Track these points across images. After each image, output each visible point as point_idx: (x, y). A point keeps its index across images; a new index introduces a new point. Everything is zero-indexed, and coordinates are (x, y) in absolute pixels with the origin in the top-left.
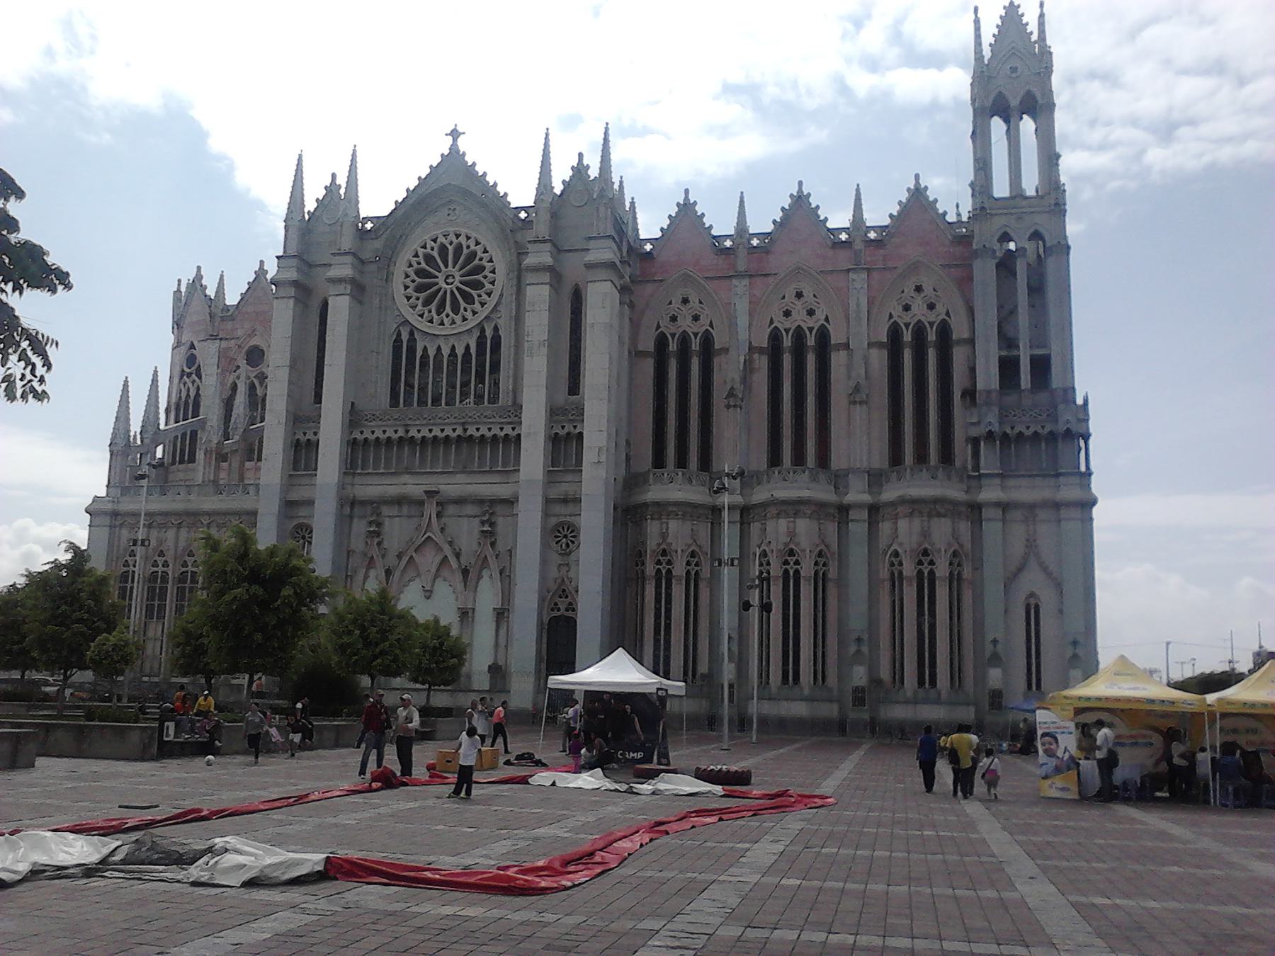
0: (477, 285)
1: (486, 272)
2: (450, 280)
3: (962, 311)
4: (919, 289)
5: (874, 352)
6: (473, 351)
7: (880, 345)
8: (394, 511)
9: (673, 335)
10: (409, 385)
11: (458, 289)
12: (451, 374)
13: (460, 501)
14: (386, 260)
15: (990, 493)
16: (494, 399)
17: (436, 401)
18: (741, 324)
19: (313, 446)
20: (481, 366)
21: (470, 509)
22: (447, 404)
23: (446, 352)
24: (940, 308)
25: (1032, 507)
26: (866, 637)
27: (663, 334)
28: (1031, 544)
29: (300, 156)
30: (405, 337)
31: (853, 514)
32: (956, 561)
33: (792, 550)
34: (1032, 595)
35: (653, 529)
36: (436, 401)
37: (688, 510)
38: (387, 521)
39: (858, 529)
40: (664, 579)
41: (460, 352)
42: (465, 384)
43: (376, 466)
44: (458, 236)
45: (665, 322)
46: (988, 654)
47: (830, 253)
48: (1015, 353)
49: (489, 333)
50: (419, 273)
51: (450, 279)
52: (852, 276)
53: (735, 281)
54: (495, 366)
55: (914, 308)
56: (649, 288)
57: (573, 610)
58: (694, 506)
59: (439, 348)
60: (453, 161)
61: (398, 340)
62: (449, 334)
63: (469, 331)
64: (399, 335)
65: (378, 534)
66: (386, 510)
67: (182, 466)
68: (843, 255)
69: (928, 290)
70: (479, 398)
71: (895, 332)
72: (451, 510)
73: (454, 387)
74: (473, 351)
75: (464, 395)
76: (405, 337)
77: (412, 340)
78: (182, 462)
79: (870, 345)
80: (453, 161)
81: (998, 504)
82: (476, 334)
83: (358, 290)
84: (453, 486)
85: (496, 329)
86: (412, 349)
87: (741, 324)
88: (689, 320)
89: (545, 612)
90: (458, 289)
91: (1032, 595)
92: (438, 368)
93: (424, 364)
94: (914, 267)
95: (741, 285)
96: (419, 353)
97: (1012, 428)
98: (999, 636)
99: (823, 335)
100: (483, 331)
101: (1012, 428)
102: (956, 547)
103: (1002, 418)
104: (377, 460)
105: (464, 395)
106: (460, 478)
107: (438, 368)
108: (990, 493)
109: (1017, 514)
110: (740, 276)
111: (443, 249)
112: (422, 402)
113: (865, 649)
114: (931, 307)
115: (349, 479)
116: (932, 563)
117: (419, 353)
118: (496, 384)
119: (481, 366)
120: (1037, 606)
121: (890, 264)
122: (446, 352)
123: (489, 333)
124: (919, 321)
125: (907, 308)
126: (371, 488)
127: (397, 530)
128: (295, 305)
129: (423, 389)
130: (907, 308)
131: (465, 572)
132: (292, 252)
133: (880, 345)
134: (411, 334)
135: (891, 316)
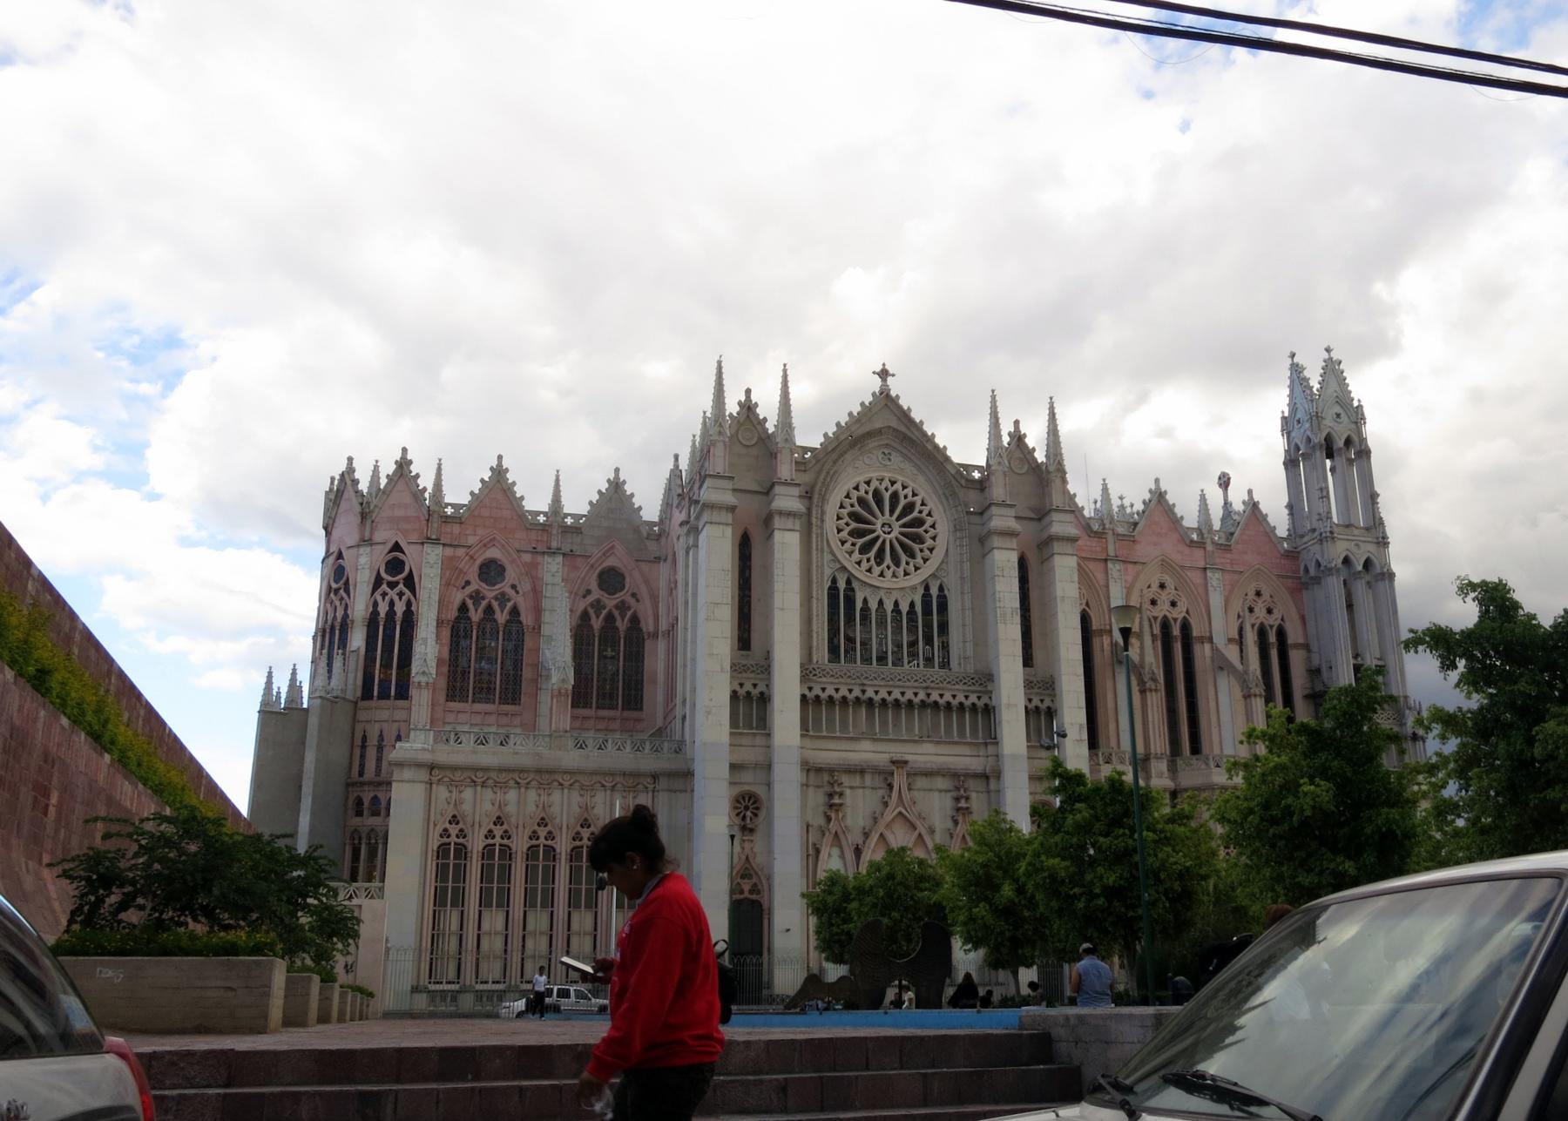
0: (918, 539)
1: (927, 526)
2: (887, 529)
3: (1296, 617)
4: (1258, 594)
6: (919, 608)
8: (856, 780)
10: (850, 640)
12: (897, 629)
13: (929, 774)
16: (945, 664)
17: (882, 659)
19: (765, 699)
20: (928, 625)
21: (941, 783)
22: (894, 664)
23: (889, 606)
24: (1277, 614)
29: (719, 363)
30: (842, 585)
38: (848, 792)
41: (904, 608)
43: (830, 727)
44: (893, 483)
47: (1187, 550)
49: (934, 592)
50: (854, 516)
51: (886, 527)
54: (944, 628)
57: (759, 892)
59: (881, 602)
60: (886, 401)
61: (833, 590)
62: (894, 587)
63: (914, 588)
64: (834, 581)
66: (846, 780)
67: (383, 703)
68: (1199, 553)
69: (1266, 594)
70: (929, 661)
72: (921, 782)
73: (899, 646)
74: (919, 608)
75: (913, 655)
76: (842, 585)
77: (850, 589)
78: (384, 695)
80: (886, 401)
82: (921, 591)
84: (924, 754)
85: (941, 588)
86: (850, 601)
88: (1167, 606)
92: (882, 623)
99: (1186, 627)
100: (927, 588)
104: (831, 721)
105: (913, 655)
106: (928, 748)
107: (882, 623)
114: (1269, 611)
117: (859, 605)
118: (945, 646)
119: (928, 625)
121: (1236, 568)
122: (889, 606)
123: (934, 592)
125: (1251, 610)
126: (831, 754)
134: (849, 582)
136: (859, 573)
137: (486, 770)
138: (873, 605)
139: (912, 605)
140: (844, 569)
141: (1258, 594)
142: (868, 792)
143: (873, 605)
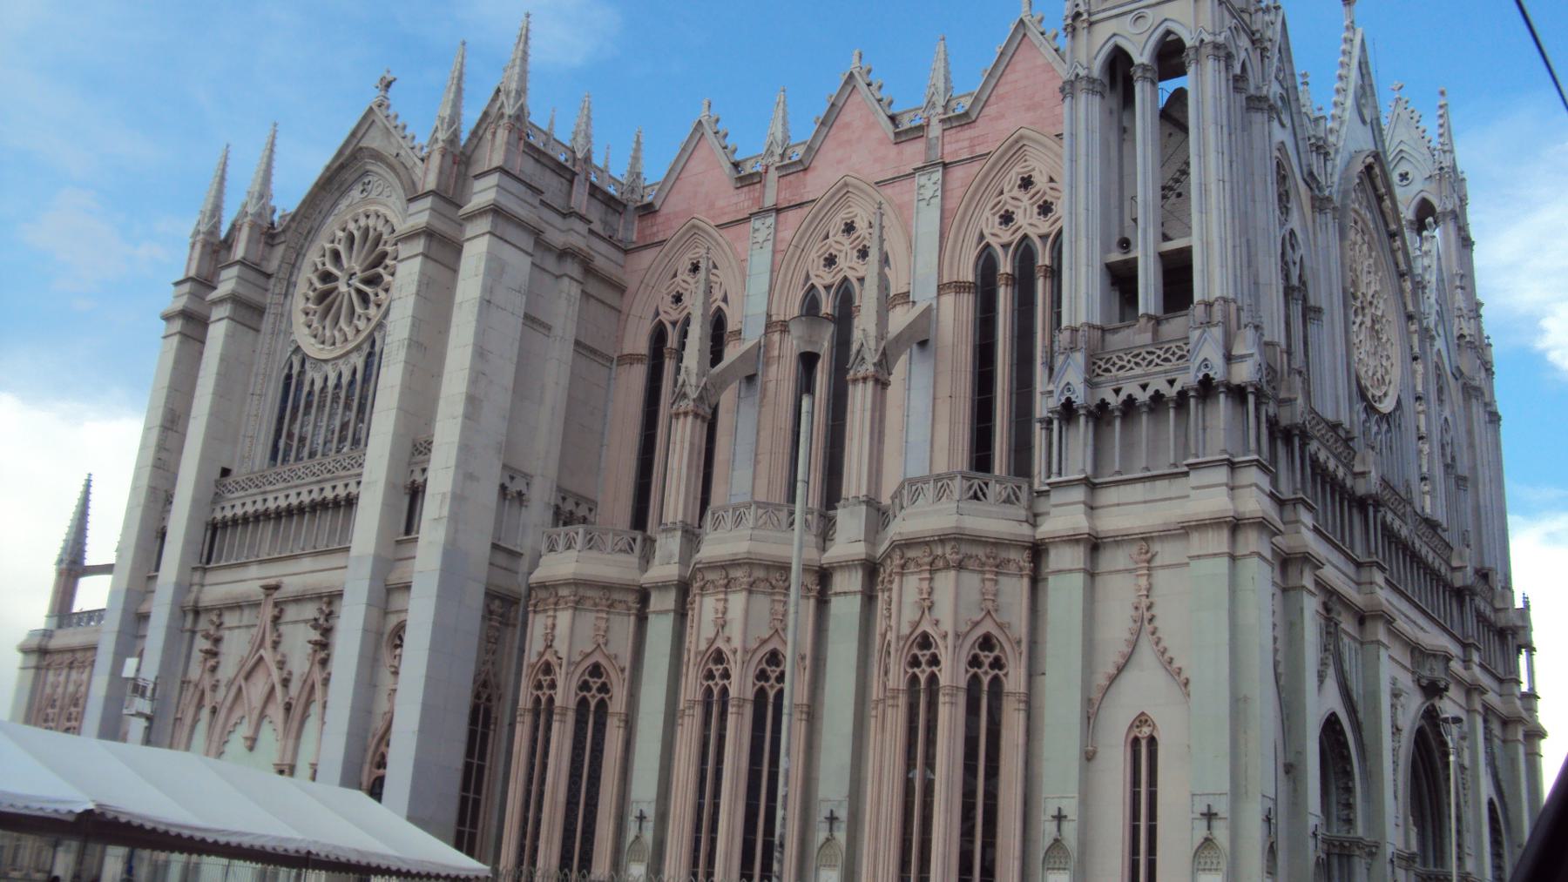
5: (948, 300)
6: (359, 376)
7: (959, 287)
9: (674, 324)
10: (290, 435)
11: (359, 291)
13: (299, 599)
14: (294, 266)
15: (1064, 516)
18: (756, 285)
21: (310, 611)
23: (331, 383)
25: (1146, 538)
26: (843, 814)
27: (661, 323)
28: (1145, 618)
31: (841, 582)
32: (987, 658)
33: (719, 652)
34: (1142, 720)
35: (538, 626)
36: (312, 455)
37: (584, 592)
39: (845, 608)
40: (543, 712)
42: (344, 426)
45: (666, 304)
46: (1047, 841)
48: (1131, 255)
52: (921, 179)
53: (756, 223)
55: (1020, 218)
56: (647, 257)
58: (607, 587)
61: (289, 377)
65: (214, 654)
69: (1040, 182)
71: (987, 263)
74: (359, 376)
77: (302, 372)
79: (942, 288)
81: (1073, 540)
83: (248, 312)
84: (300, 575)
87: (756, 285)
89: (366, 768)
90: (359, 291)
91: (1142, 720)
92: (321, 407)
93: (309, 405)
94: (1017, 147)
95: (764, 226)
96: (306, 389)
97: (1117, 391)
98: (1071, 808)
101: (1117, 391)
102: (988, 627)
103: (1094, 371)
108: (1064, 516)
109: (1114, 559)
110: (762, 212)
111: (351, 238)
112: (298, 458)
113: (841, 836)
114: (1045, 209)
115: (197, 577)
116: (997, 664)
117: (306, 389)
120: (1152, 741)
121: (980, 150)
124: (1025, 237)
125: (1007, 218)
127: (236, 646)
128: (181, 342)
129: (302, 440)
130: (1007, 218)
131: (288, 708)
132: (192, 273)
133: (959, 287)
135: (982, 237)
136: (312, 348)
137: (73, 650)
138: (317, 387)
139: (354, 372)
140: (298, 349)
141: (1026, 183)
142: (243, 631)
143: (317, 387)
